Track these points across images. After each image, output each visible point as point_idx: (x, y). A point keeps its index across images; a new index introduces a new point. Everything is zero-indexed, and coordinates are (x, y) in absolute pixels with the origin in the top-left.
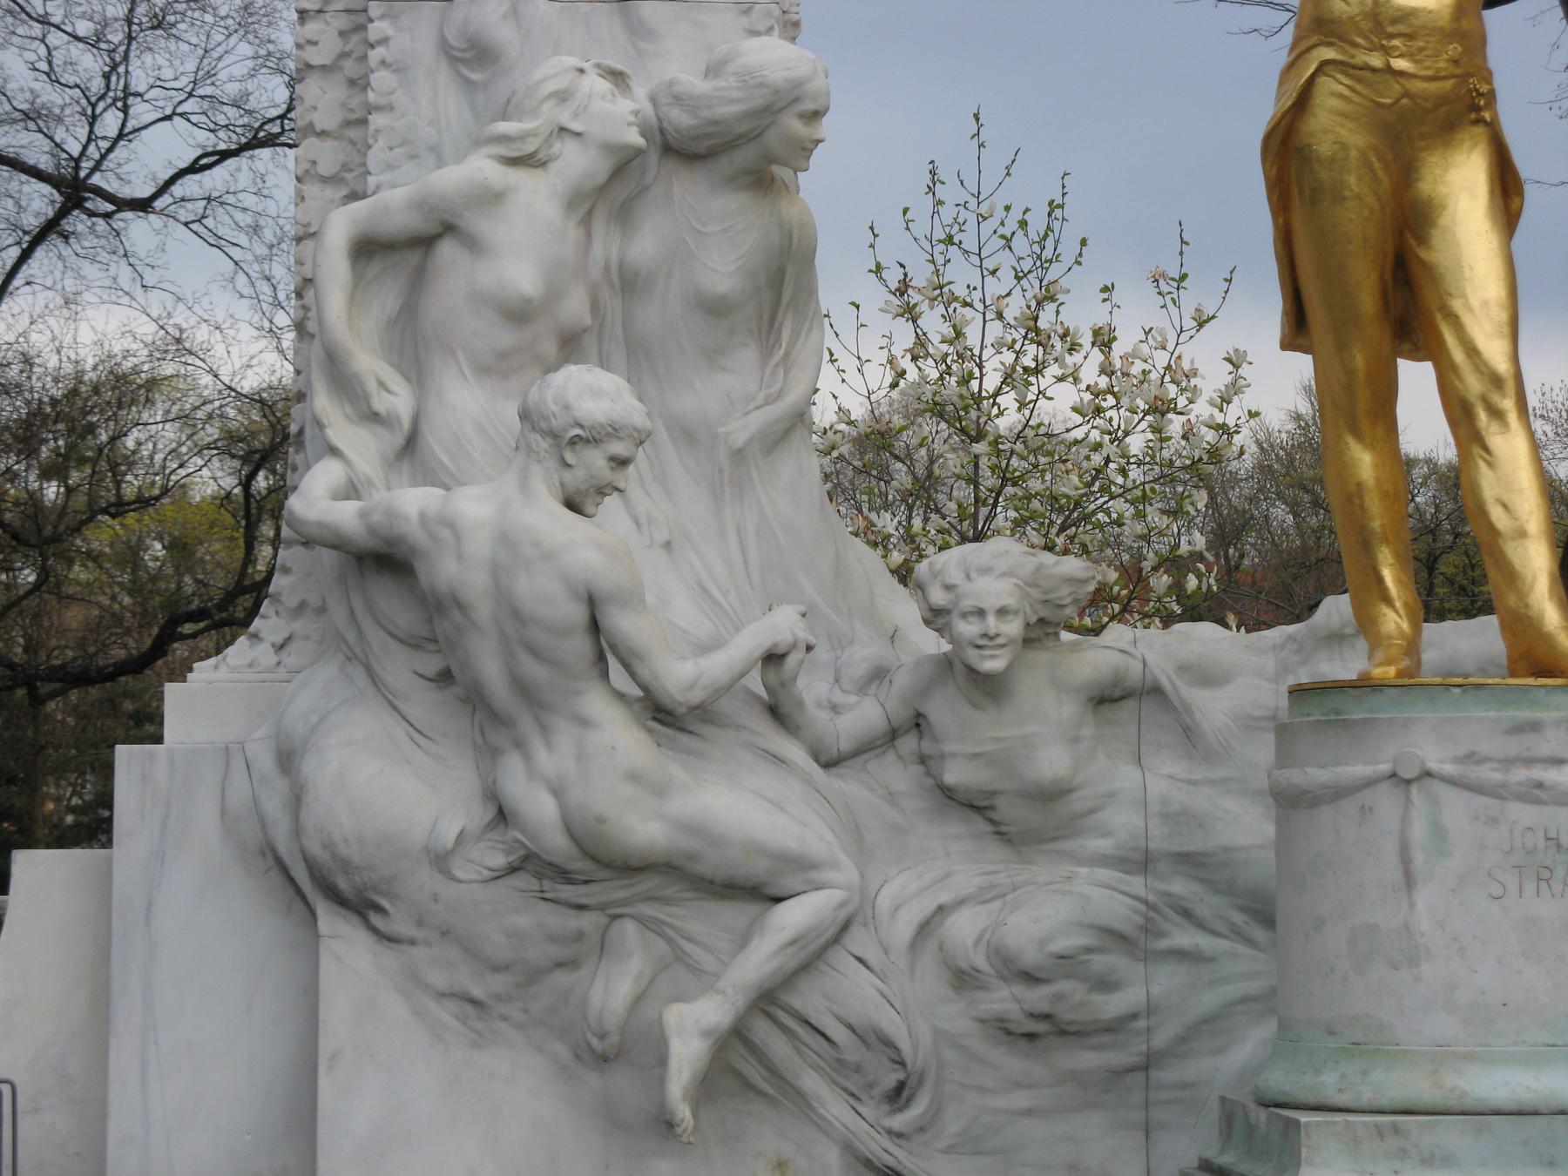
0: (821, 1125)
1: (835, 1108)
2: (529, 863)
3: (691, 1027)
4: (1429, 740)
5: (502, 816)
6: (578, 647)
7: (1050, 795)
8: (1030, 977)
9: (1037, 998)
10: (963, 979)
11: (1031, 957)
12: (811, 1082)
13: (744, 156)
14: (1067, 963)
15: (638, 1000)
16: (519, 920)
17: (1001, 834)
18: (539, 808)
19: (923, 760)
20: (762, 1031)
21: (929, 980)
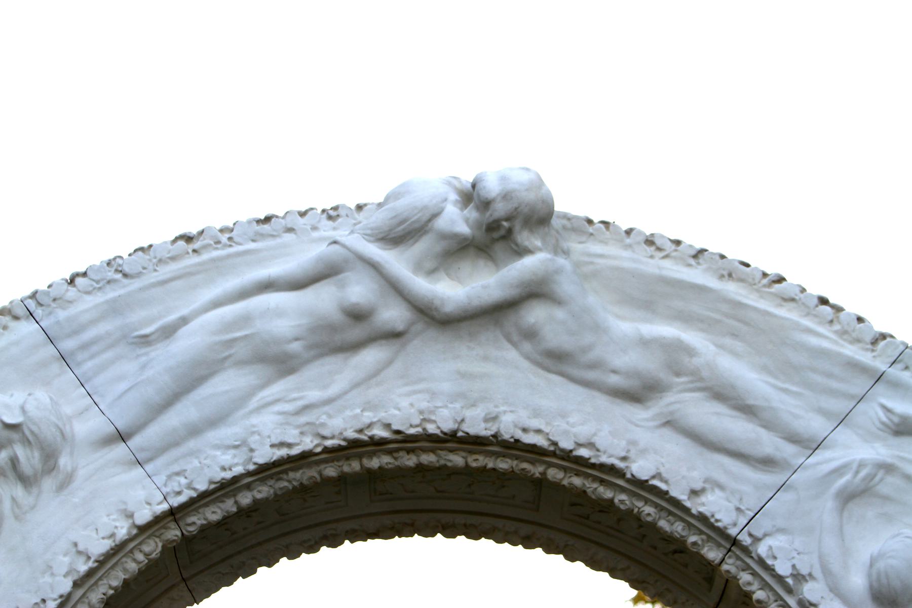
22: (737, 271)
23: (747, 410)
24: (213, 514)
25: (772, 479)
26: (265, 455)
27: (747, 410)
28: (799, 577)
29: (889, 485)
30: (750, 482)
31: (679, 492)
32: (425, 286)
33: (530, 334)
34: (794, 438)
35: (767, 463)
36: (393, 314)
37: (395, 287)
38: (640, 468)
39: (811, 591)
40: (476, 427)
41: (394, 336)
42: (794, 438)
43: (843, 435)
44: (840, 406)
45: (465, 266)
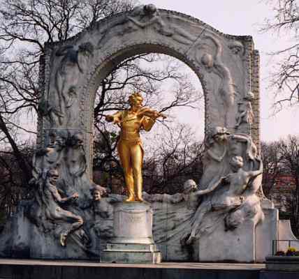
0: (79, 246)
1: (81, 245)
2: (47, 219)
3: (63, 236)
4: (122, 207)
5: (46, 214)
6: (50, 197)
7: (106, 213)
8: (103, 232)
9: (104, 234)
10: (96, 232)
11: (102, 230)
12: (78, 242)
13: (75, 147)
14: (106, 230)
15: (61, 232)
16: (48, 225)
17: (101, 216)
18: (48, 213)
19: (93, 209)
20: (72, 236)
21: (92, 231)
22: (183, 15)
23: (185, 37)
24: (113, 57)
25: (188, 47)
26: (119, 49)
27: (185, 37)
28: (193, 61)
29: (204, 46)
30: (184, 47)
31: (176, 49)
32: (138, 23)
33: (155, 28)
34: (192, 41)
35: (188, 44)
36: (135, 27)
37: (135, 23)
38: (171, 47)
39: (194, 63)
40: (148, 42)
41: (135, 30)
42: (192, 41)
43: (199, 39)
44: (198, 35)
45: (144, 19)
